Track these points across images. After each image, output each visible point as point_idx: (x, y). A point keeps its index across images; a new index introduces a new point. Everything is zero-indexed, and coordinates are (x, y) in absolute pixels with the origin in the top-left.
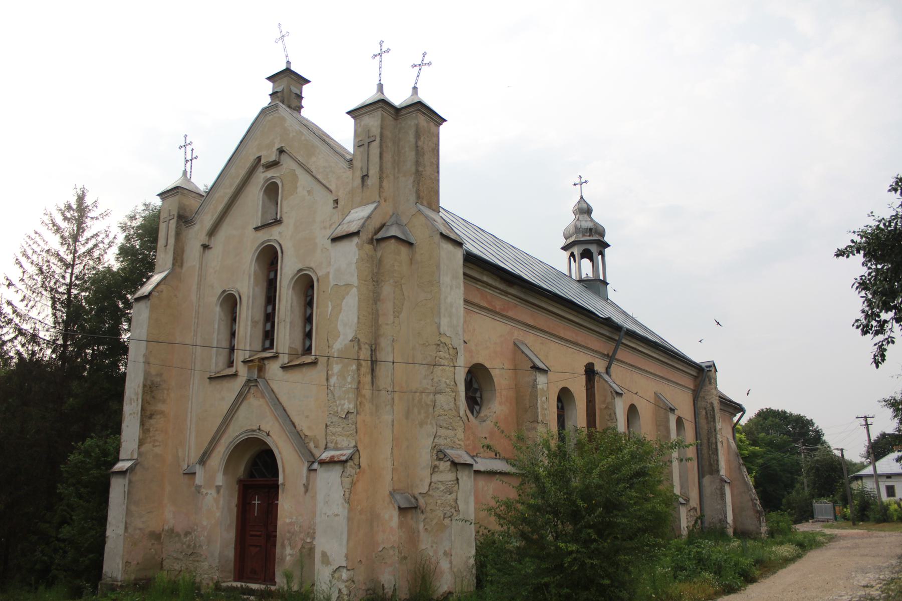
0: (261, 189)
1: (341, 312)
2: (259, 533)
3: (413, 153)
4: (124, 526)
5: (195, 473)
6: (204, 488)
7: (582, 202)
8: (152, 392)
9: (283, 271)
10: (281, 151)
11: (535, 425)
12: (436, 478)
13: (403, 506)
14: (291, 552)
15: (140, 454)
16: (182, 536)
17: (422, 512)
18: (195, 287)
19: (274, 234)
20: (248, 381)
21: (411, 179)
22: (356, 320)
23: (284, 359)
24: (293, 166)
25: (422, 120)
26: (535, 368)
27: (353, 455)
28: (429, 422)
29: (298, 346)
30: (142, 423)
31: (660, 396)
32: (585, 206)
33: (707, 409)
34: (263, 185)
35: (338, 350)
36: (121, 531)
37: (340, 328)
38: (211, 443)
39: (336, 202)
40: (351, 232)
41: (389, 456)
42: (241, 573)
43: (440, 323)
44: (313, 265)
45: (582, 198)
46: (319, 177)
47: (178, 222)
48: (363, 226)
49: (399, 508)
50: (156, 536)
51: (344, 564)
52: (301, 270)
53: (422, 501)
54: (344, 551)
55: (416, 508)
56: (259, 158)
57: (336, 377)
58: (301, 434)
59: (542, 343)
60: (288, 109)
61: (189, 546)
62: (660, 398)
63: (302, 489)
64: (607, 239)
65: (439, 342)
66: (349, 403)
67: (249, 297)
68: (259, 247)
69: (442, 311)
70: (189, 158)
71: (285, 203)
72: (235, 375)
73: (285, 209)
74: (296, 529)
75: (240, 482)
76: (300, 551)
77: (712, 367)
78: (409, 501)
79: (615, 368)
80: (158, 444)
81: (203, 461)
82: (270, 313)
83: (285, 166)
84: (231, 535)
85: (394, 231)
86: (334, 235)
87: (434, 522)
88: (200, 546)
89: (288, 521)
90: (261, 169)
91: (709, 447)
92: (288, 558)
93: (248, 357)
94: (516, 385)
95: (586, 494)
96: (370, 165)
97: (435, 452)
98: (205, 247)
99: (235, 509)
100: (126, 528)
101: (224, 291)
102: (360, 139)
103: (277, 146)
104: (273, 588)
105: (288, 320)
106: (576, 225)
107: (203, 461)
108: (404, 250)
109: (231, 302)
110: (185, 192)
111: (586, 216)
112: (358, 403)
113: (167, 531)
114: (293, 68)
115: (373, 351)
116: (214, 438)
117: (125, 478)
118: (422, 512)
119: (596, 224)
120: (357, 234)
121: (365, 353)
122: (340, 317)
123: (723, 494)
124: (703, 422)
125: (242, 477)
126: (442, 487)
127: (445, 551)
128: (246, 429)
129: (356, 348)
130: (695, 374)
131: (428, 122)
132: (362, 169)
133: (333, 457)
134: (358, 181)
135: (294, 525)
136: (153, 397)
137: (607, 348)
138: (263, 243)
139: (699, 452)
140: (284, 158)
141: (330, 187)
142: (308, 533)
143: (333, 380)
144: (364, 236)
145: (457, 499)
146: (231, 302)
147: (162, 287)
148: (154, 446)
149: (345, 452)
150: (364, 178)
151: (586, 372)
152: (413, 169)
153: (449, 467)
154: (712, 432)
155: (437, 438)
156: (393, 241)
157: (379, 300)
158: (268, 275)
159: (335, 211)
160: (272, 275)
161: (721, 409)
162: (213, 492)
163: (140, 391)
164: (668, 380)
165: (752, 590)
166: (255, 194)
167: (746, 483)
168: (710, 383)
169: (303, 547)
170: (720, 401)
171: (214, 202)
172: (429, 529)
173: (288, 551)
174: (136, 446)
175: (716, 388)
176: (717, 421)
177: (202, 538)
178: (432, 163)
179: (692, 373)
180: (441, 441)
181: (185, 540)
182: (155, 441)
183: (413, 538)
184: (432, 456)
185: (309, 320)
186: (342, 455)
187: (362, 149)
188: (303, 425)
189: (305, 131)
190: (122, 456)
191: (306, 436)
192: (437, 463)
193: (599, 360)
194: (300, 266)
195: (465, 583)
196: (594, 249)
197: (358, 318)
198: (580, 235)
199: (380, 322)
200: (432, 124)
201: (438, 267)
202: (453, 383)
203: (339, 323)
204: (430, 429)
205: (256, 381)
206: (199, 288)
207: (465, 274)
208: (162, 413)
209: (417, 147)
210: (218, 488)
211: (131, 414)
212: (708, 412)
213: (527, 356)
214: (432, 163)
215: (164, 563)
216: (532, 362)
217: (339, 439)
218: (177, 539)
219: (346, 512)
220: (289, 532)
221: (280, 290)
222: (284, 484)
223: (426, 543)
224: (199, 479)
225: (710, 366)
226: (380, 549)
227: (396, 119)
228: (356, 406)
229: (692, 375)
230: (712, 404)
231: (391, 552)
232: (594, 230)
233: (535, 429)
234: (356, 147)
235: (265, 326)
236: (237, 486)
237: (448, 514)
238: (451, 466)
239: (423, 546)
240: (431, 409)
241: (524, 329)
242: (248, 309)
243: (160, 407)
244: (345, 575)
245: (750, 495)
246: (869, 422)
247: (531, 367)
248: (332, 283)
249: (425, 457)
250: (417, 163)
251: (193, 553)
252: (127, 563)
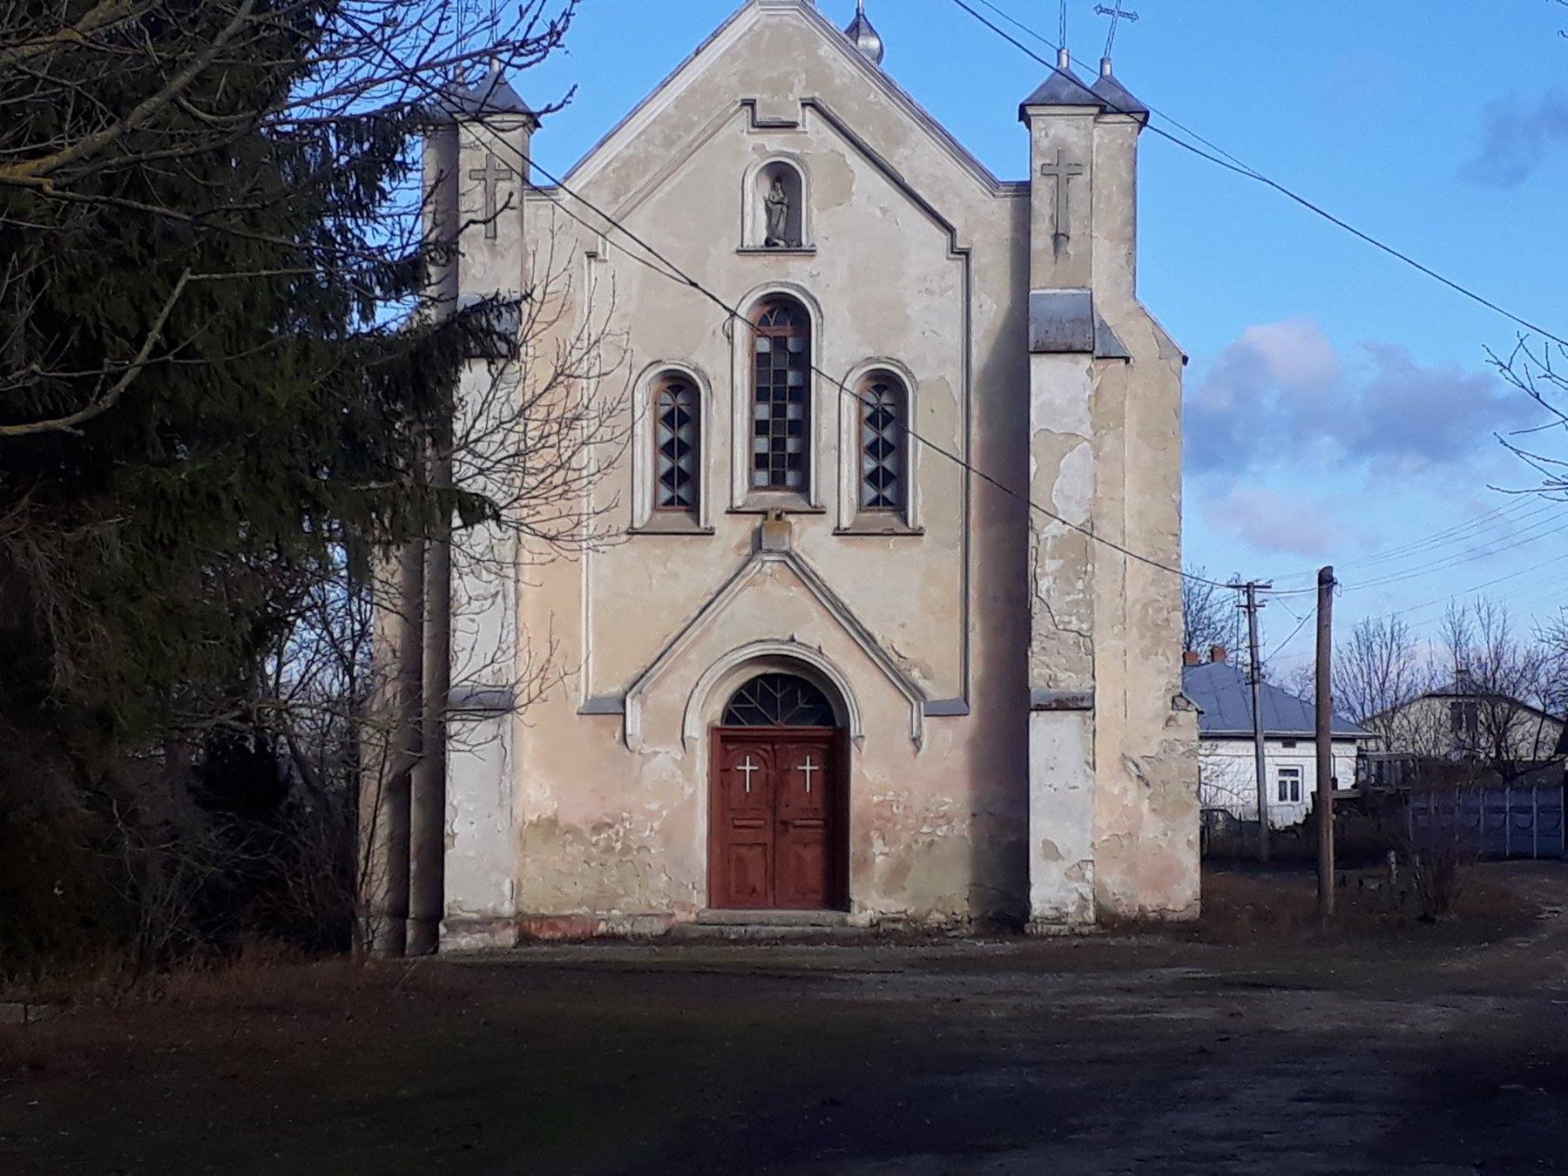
14: (886, 850)
16: (587, 834)
43: (1181, 502)
44: (900, 356)
46: (919, 192)
51: (1091, 858)
52: (869, 360)
57: (1051, 579)
58: (890, 653)
63: (910, 748)
75: (713, 730)
92: (879, 859)
102: (1048, 161)
125: (718, 724)
135: (892, 806)
158: (753, 345)
173: (878, 846)
181: (594, 839)
187: (1052, 181)
192: (1173, 713)
194: (870, 353)
218: (569, 837)
220: (880, 817)
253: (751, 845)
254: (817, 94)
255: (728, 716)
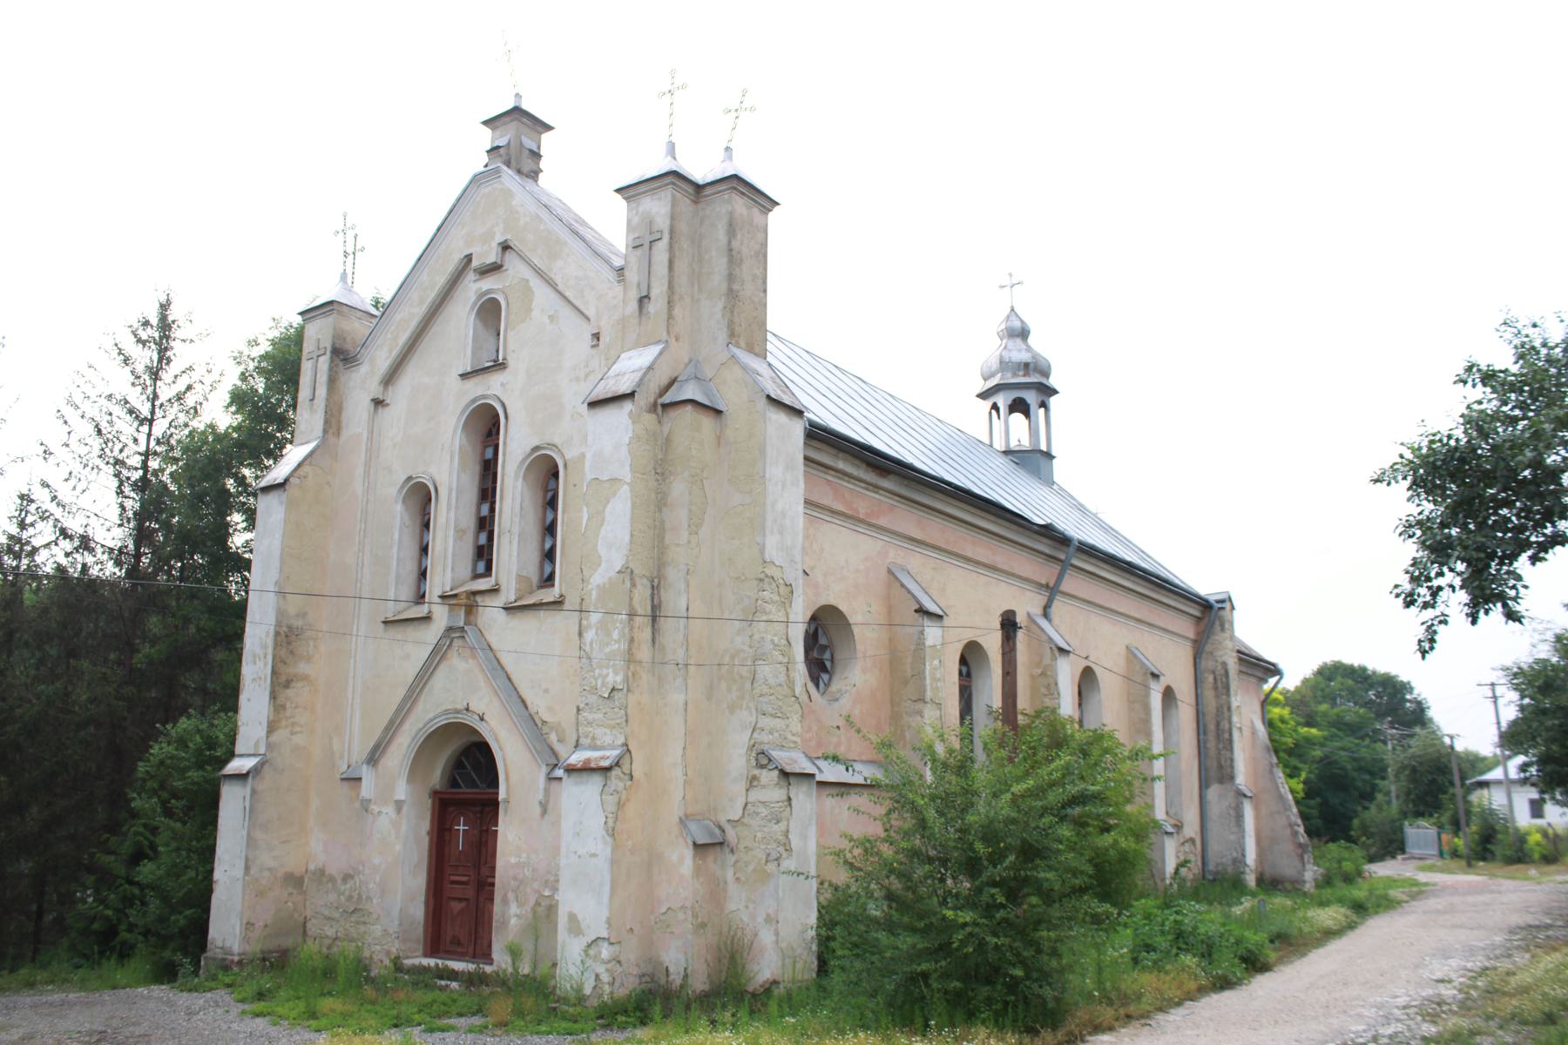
0: (472, 309)
1: (602, 525)
2: (464, 879)
3: (725, 260)
4: (243, 865)
5: (360, 779)
6: (375, 804)
7: (1014, 318)
8: (289, 643)
9: (509, 449)
10: (506, 247)
11: (919, 706)
12: (755, 795)
13: (700, 842)
14: (518, 911)
15: (269, 746)
16: (339, 882)
17: (732, 851)
18: (360, 470)
19: (493, 387)
20: (450, 629)
21: (720, 305)
22: (627, 538)
23: (509, 594)
24: (526, 272)
25: (739, 205)
26: (922, 611)
27: (621, 757)
28: (744, 706)
29: (533, 574)
30: (273, 696)
31: (1136, 652)
32: (1017, 324)
33: (1217, 673)
34: (475, 304)
35: (598, 586)
36: (239, 872)
37: (602, 550)
38: (387, 729)
39: (597, 336)
40: (620, 393)
41: (679, 761)
42: (436, 943)
43: (764, 544)
44: (556, 441)
45: (1012, 310)
46: (567, 294)
47: (332, 361)
48: (640, 383)
49: (695, 844)
50: (295, 881)
51: (605, 935)
52: (537, 448)
53: (731, 834)
54: (605, 914)
55: (721, 844)
56: (469, 258)
57: (594, 630)
59: (934, 569)
60: (517, 177)
61: (350, 898)
62: (1135, 656)
63: (538, 810)
64: (1053, 381)
65: (762, 576)
66: (616, 673)
67: (450, 490)
68: (467, 406)
69: (769, 523)
70: (350, 250)
71: (511, 334)
72: (427, 619)
73: (512, 345)
74: (527, 873)
75: (435, 794)
76: (534, 912)
77: (1226, 602)
78: (711, 834)
79: (1059, 607)
80: (298, 729)
81: (373, 758)
82: (485, 517)
83: (511, 272)
84: (418, 882)
85: (690, 392)
86: (593, 397)
87: (751, 867)
88: (369, 898)
89: (513, 860)
90: (471, 276)
91: (1218, 736)
92: (513, 921)
93: (448, 589)
94: (890, 640)
95: (990, 834)
96: (653, 279)
97: (754, 754)
98: (378, 403)
99: (426, 840)
100: (247, 868)
101: (410, 478)
102: (636, 235)
103: (499, 238)
104: (488, 969)
105: (516, 530)
106: (1001, 357)
107: (373, 758)
108: (707, 421)
109: (421, 498)
110: (345, 309)
111: (1019, 341)
112: (630, 674)
113: (314, 873)
114: (525, 106)
115: (655, 589)
116: (392, 722)
117: (245, 786)
118: (732, 851)
119: (1035, 356)
120: (630, 395)
121: (642, 594)
122: (603, 532)
123: (1239, 817)
124: (1209, 694)
125: (438, 787)
126: (764, 811)
127: (768, 915)
128: (444, 708)
129: (628, 583)
130: (1197, 613)
131: (749, 208)
132: (639, 285)
133: (588, 761)
134: (633, 306)
136: (292, 652)
137: (1047, 573)
138: (474, 401)
139: (1202, 745)
140: (509, 255)
141: (586, 312)
142: (546, 881)
143: (589, 635)
144: (643, 399)
145: (788, 831)
146: (421, 498)
147: (306, 469)
148: (292, 733)
149: (608, 753)
150: (643, 300)
151: (1003, 625)
152: (724, 287)
153: (776, 779)
154: (1224, 711)
155: (758, 731)
156: (689, 408)
157: (665, 505)
158: (483, 454)
159: (594, 351)
160: (489, 454)
161: (1241, 672)
162: (390, 810)
163: (270, 642)
164: (1150, 625)
165: (1262, 987)
166: (461, 318)
167: (1281, 797)
168: (1223, 629)
169: (538, 904)
170: (1240, 659)
171: (393, 328)
172: (743, 879)
173: (514, 909)
174: (264, 734)
175: (1232, 637)
176: (1232, 692)
177: (371, 886)
178: (754, 277)
179: (1192, 611)
180: (765, 737)
181: (343, 888)
182: (293, 724)
183: (716, 894)
184: (748, 761)
185: (550, 529)
186: (602, 758)
187: (639, 252)
188: (538, 703)
189: (544, 214)
190: (239, 749)
191: (544, 722)
192: (756, 772)
193: (1032, 594)
194: (536, 442)
195: (799, 965)
196: (1031, 398)
197: (632, 535)
198: (1009, 375)
199: (667, 541)
200: (756, 211)
201: (762, 451)
202: (784, 642)
203: (600, 542)
204: (746, 716)
205: (462, 629)
206: (367, 473)
207: (806, 458)
208: (305, 678)
209: (731, 250)
210: (399, 805)
211: (254, 680)
212: (1219, 678)
213: (909, 592)
214: (754, 277)
215: (309, 925)
216: (918, 602)
217: (599, 731)
218: (330, 885)
219: (609, 850)
220: (515, 879)
221: (503, 480)
222: (507, 801)
223: (737, 902)
224: (367, 789)
225: (1222, 601)
226: (663, 910)
227: (696, 202)
228: (626, 679)
229: (1191, 615)
230: (1224, 664)
231: (681, 916)
232: (1031, 366)
233: (920, 713)
234: (630, 249)
235: (477, 537)
236: (430, 801)
237: (774, 855)
238: (779, 777)
239: (731, 906)
240: (748, 685)
241: (906, 545)
242: (449, 510)
243: (303, 668)
244: (605, 952)
245: (1288, 817)
246: (1498, 694)
247: (916, 611)
248: (589, 476)
249: (738, 761)
250: (731, 277)
251: (356, 910)
252: (249, 925)
253: (460, 900)
254: (509, 237)
255: (453, 783)
